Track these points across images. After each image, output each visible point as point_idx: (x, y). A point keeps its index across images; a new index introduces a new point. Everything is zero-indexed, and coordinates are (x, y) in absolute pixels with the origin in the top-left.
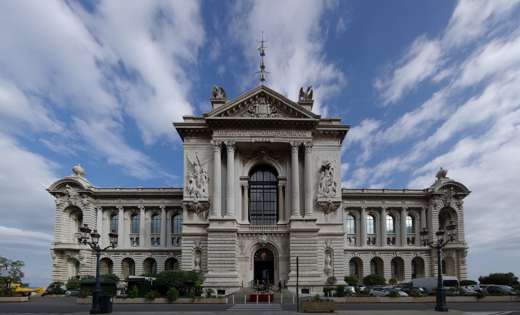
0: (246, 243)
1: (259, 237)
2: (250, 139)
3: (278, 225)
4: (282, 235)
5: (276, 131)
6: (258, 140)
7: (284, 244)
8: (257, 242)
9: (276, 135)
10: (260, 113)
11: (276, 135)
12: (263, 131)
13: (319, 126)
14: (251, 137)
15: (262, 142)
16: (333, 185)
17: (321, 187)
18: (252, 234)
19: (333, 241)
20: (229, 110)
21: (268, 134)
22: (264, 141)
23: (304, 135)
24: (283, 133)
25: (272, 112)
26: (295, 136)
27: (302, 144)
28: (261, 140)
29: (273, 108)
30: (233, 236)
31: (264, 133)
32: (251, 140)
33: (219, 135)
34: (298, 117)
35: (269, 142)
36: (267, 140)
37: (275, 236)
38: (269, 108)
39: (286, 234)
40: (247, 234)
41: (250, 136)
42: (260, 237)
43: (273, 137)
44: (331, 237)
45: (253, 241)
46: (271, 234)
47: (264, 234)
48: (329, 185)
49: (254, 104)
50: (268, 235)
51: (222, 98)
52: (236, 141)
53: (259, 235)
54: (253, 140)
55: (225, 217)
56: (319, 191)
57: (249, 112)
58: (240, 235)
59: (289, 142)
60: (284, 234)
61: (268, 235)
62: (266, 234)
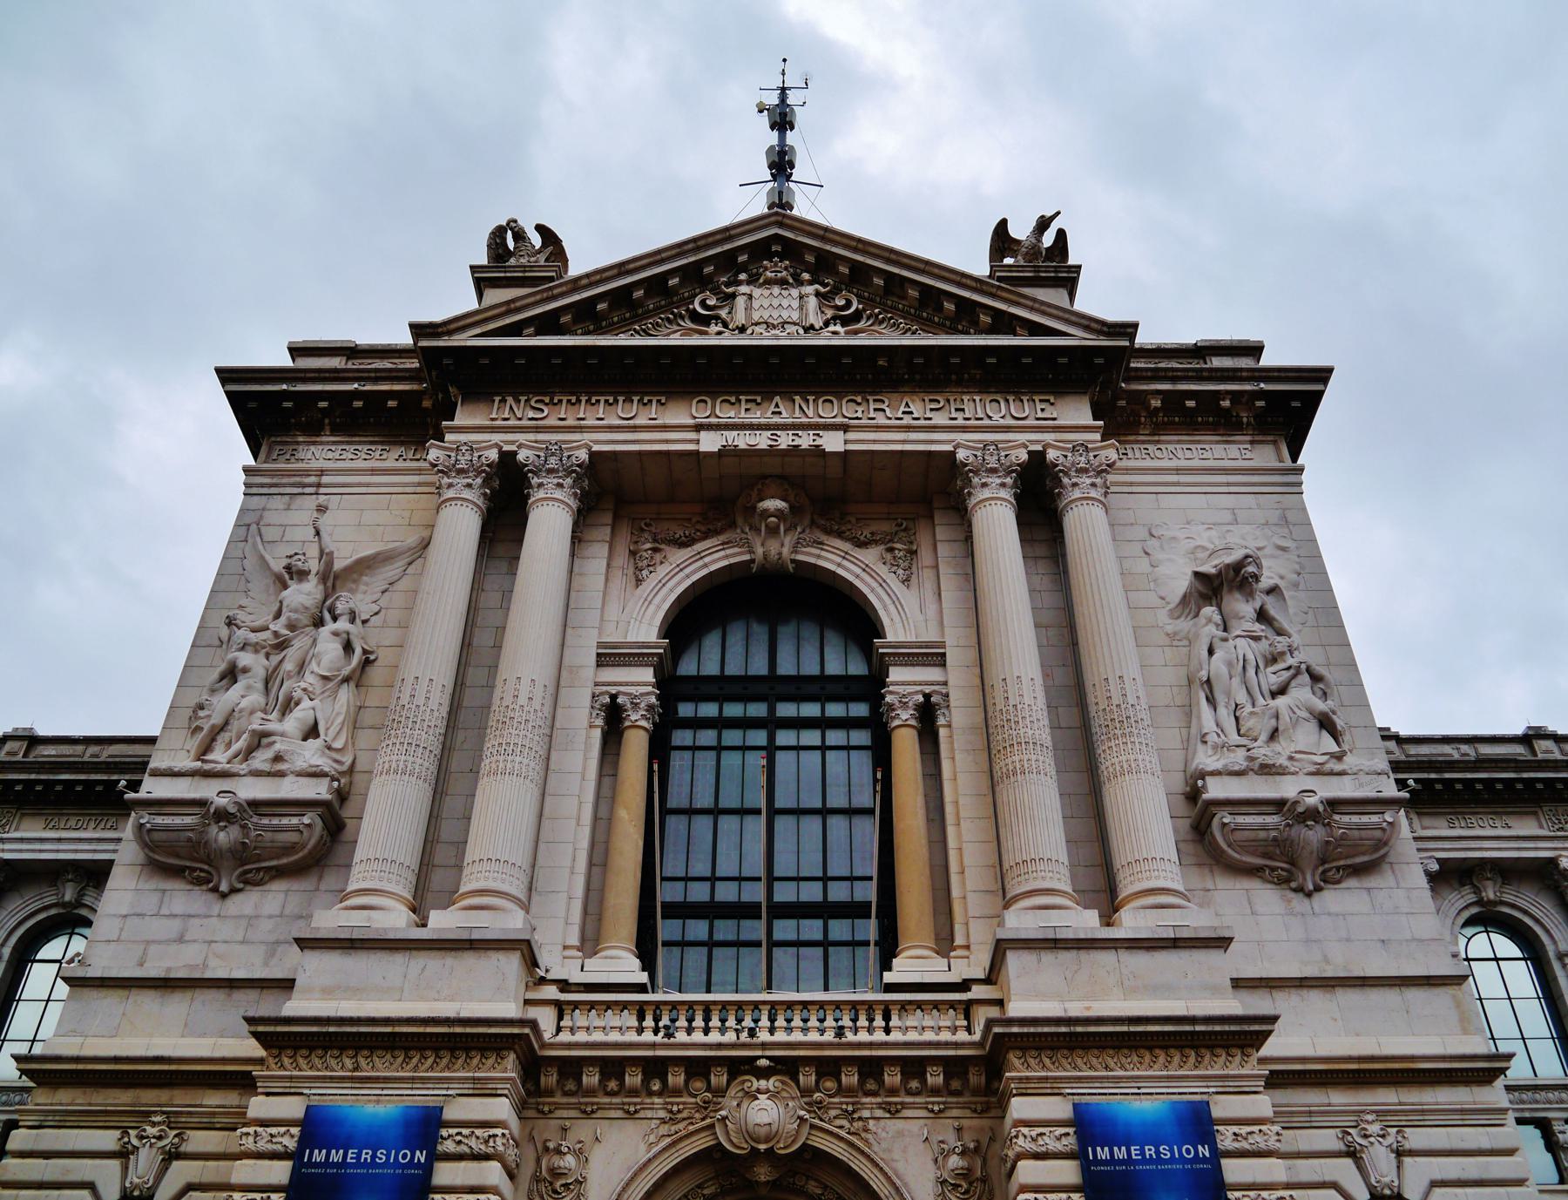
0: (597, 1156)
1: (721, 1092)
2: (693, 435)
3: (890, 988)
4: (935, 1078)
5: (859, 399)
6: (743, 440)
7: (955, 1161)
8: (700, 1143)
9: (857, 418)
10: (756, 317)
11: (857, 418)
12: (777, 399)
13: (1133, 374)
14: (698, 428)
15: (772, 452)
16: (1302, 693)
17: (1211, 701)
18: (655, 1068)
19: (1417, 1138)
20: (573, 310)
21: (810, 413)
22: (783, 446)
23: (1040, 415)
24: (902, 409)
25: (834, 318)
26: (986, 422)
27: (1037, 458)
28: (762, 441)
29: (840, 302)
30: (483, 1090)
31: (782, 409)
32: (698, 442)
33: (493, 419)
34: (992, 330)
35: (818, 452)
36: (805, 440)
37: (871, 1085)
38: (812, 302)
39: (972, 1070)
40: (612, 1068)
41: (691, 422)
42: (732, 1092)
43: (845, 428)
44: (1387, 1097)
45: (664, 1129)
46: (828, 1067)
47: (763, 1062)
48: (1274, 688)
49: (728, 285)
50: (807, 1078)
51: (542, 263)
52: (596, 448)
53: (719, 1078)
54: (710, 443)
55: (442, 922)
56: (1200, 727)
57: (695, 317)
58: (550, 1079)
59: (949, 448)
60: (955, 1067)
61: (807, 1078)
62: (786, 1067)
